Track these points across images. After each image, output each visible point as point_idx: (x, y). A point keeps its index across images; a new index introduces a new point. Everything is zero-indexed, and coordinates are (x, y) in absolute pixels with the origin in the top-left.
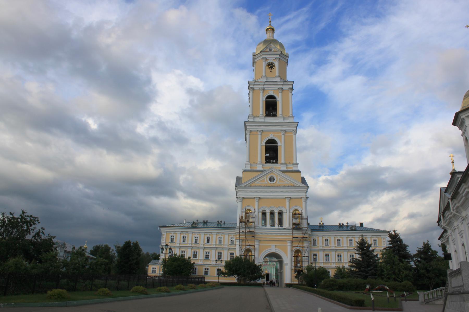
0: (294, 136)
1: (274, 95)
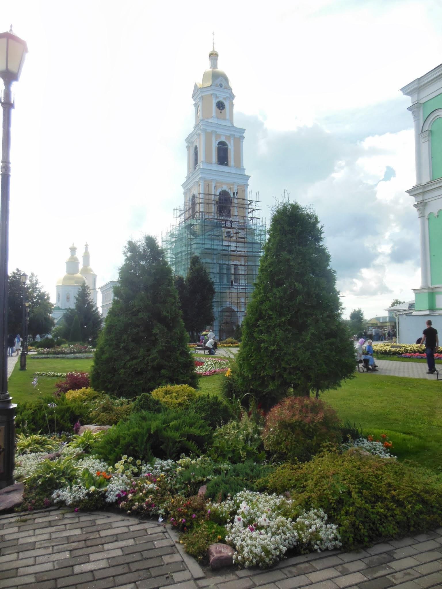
1: (226, 141)
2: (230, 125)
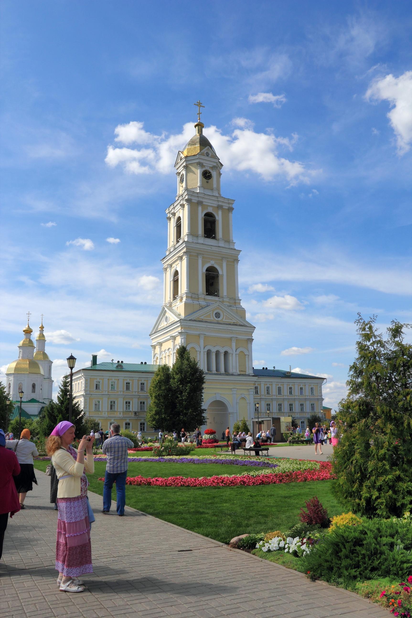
0: (236, 266)
2: (217, 195)
